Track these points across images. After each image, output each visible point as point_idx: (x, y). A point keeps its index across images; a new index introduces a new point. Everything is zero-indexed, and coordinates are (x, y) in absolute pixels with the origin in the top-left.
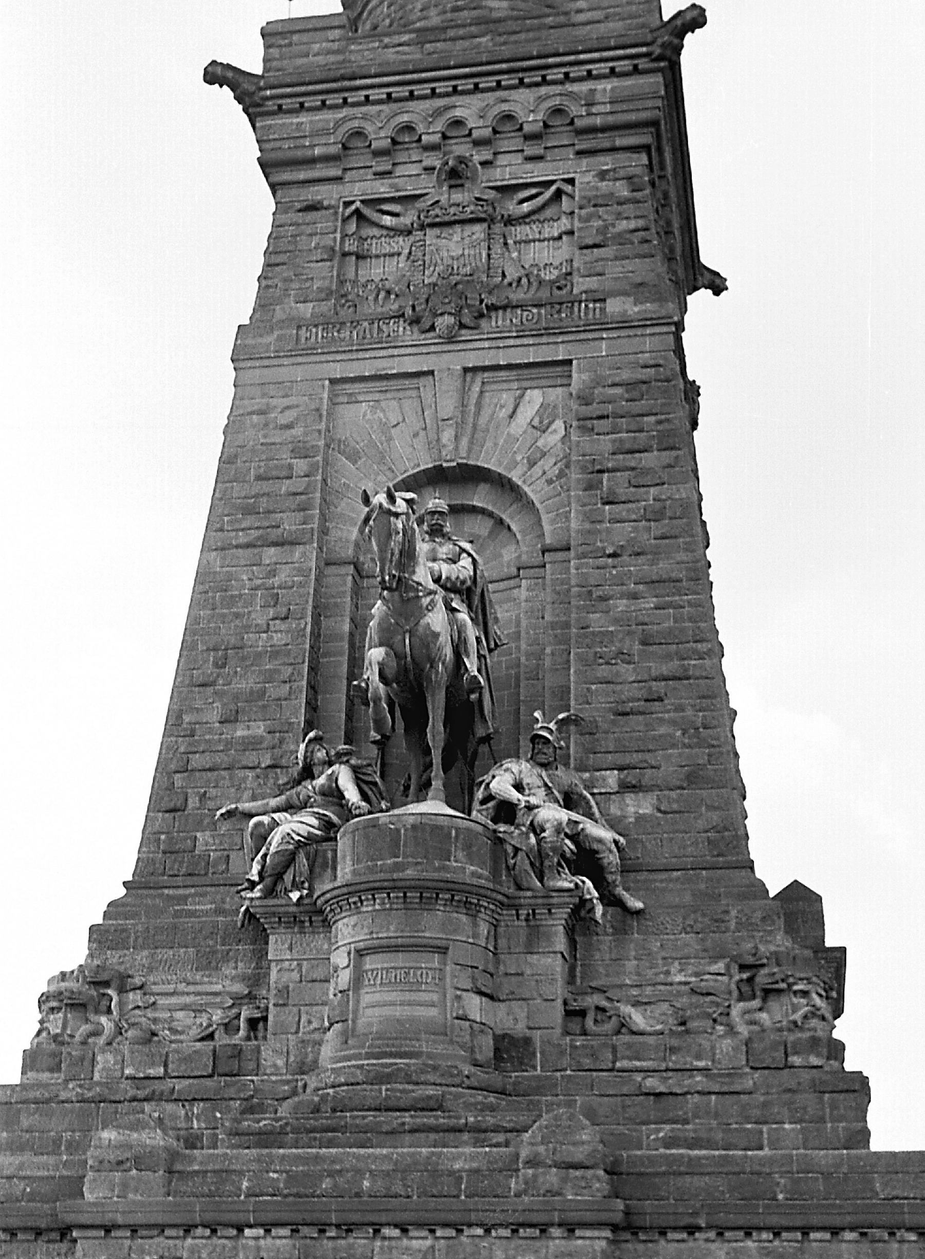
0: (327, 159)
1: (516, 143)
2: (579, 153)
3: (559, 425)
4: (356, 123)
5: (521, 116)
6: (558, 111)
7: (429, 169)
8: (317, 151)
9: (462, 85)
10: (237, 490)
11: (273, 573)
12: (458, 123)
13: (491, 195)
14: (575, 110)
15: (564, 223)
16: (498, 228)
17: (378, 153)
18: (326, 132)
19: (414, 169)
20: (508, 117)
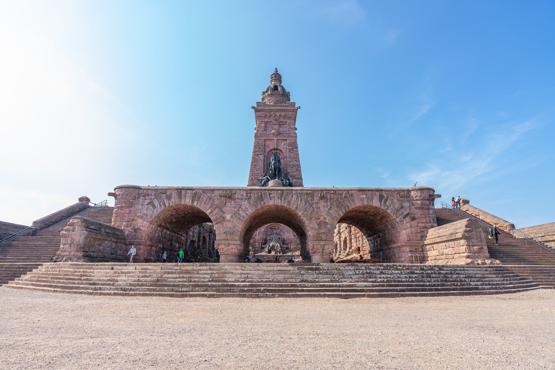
0: (263, 117)
1: (281, 117)
2: (288, 119)
3: (286, 145)
4: (265, 114)
5: (282, 115)
6: (286, 115)
7: (273, 119)
8: (262, 116)
12: (276, 115)
13: (279, 122)
14: (287, 115)
15: (286, 126)
17: (268, 117)
18: (263, 114)
19: (271, 119)
20: (281, 115)
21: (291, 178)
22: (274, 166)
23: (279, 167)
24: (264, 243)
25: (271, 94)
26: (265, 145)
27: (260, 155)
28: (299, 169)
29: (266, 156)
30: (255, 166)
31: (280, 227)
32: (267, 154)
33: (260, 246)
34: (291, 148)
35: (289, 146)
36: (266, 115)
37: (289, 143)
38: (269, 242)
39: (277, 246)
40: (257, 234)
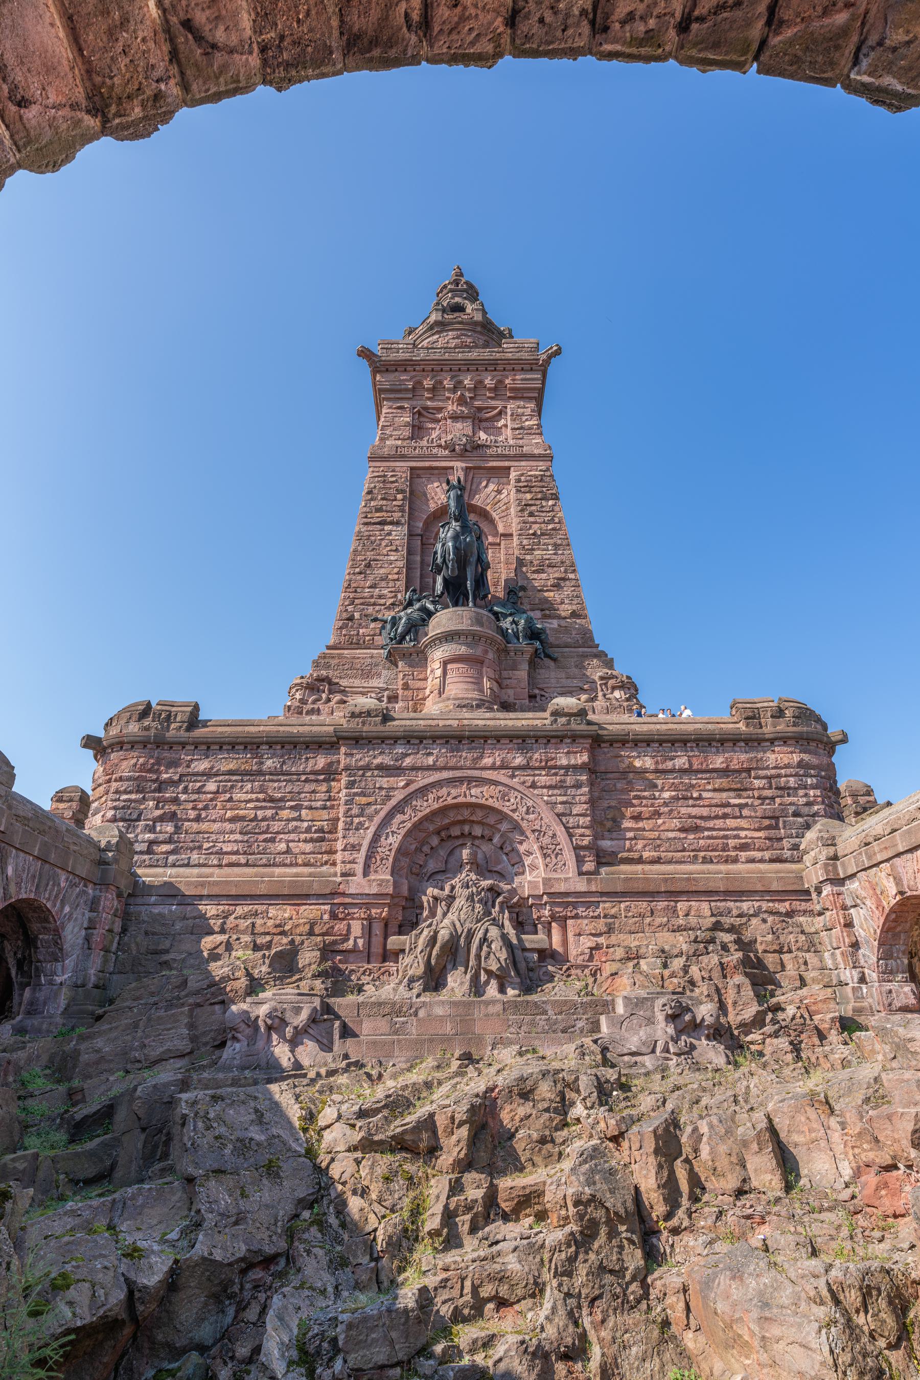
0: (407, 390)
9: (465, 368)
10: (373, 503)
11: (389, 534)
16: (477, 422)
17: (428, 390)
18: (406, 380)
21: (538, 614)
22: (455, 548)
23: (480, 560)
24: (400, 926)
25: (437, 323)
26: (412, 492)
27: (391, 523)
28: (572, 576)
29: (419, 532)
30: (368, 566)
31: (500, 821)
32: (421, 525)
33: (377, 940)
34: (528, 496)
35: (518, 491)
36: (418, 386)
37: (519, 481)
38: (433, 914)
39: (484, 939)
40: (359, 868)
